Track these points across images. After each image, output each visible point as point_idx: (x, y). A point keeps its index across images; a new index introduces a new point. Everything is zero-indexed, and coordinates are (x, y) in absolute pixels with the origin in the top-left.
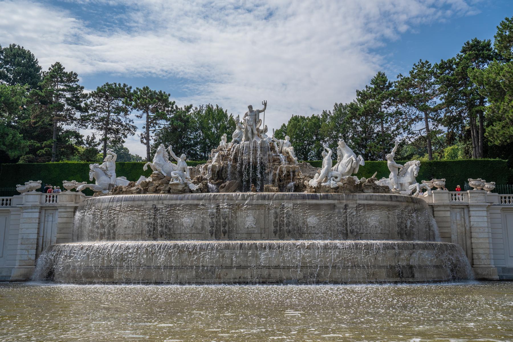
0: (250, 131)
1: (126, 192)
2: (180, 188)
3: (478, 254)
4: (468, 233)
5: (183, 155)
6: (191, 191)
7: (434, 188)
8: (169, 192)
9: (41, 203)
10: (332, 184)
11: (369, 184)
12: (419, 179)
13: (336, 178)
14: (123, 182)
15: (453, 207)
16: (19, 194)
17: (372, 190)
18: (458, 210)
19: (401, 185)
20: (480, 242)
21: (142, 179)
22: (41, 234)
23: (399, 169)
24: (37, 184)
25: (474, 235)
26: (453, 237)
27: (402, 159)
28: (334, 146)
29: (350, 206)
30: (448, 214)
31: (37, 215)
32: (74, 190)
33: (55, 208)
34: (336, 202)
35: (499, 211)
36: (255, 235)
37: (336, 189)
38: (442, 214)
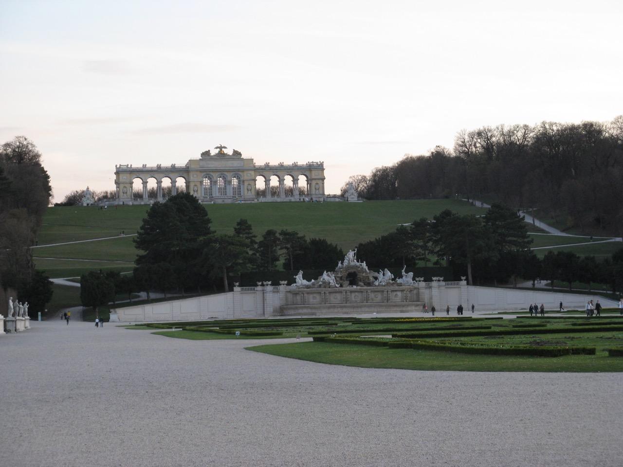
1: (312, 288)
4: (431, 298)
6: (336, 287)
7: (420, 281)
10: (384, 284)
12: (414, 279)
14: (305, 282)
16: (258, 286)
17: (396, 285)
21: (313, 281)
24: (270, 283)
28: (383, 271)
30: (424, 291)
32: (284, 285)
33: (278, 292)
37: (384, 286)
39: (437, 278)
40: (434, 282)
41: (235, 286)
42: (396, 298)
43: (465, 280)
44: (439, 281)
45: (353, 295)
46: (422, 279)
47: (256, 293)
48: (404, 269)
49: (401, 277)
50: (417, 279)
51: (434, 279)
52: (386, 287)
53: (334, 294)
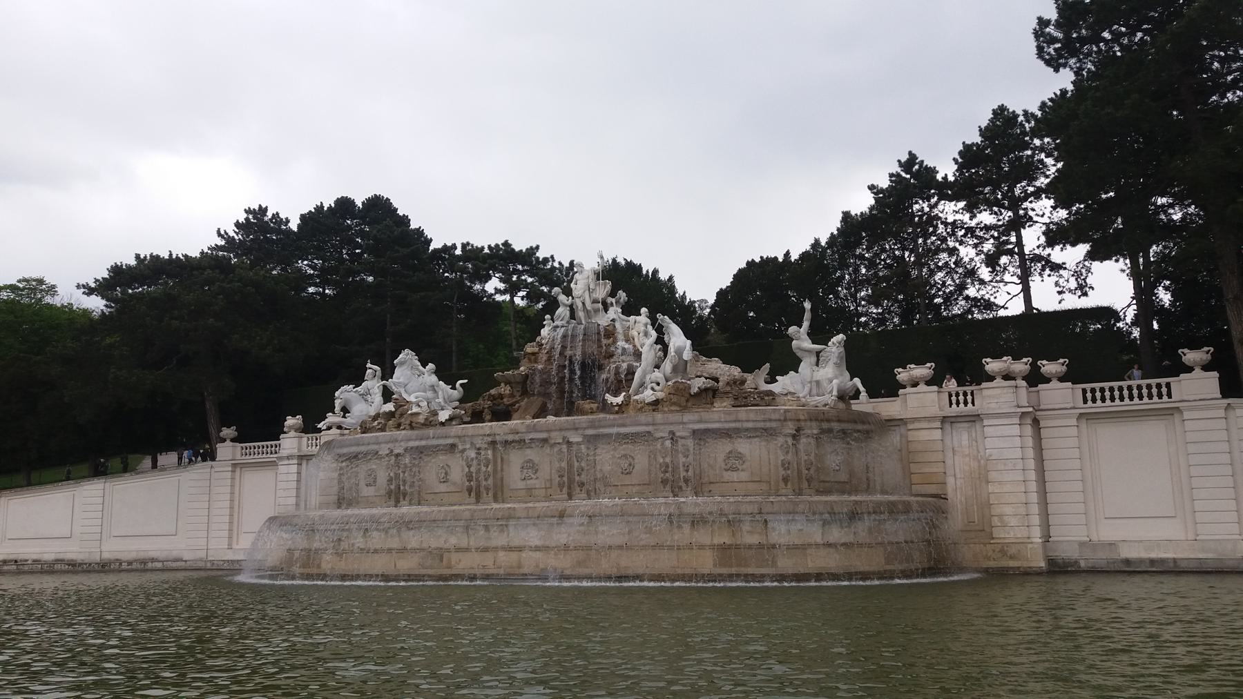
0: (580, 305)
2: (421, 419)
3: (1000, 516)
4: (981, 476)
5: (431, 366)
6: (442, 424)
8: (412, 428)
9: (299, 450)
10: (648, 395)
11: (728, 389)
13: (658, 384)
15: (944, 419)
18: (966, 425)
19: (818, 383)
20: (1005, 490)
22: (303, 498)
23: (818, 353)
25: (993, 475)
26: (950, 481)
27: (819, 335)
29: (678, 434)
30: (937, 434)
31: (294, 468)
34: (650, 428)
35: (1074, 422)
36: (536, 492)
37: (656, 403)
38: (924, 435)
39: (1022, 366)
40: (999, 382)
41: (224, 440)
42: (728, 476)
43: (1206, 368)
44: (1035, 378)
45: (515, 459)
46: (924, 371)
47: (273, 464)
48: (806, 324)
49: (789, 363)
50: (902, 375)
51: (992, 365)
52: (659, 417)
53: (442, 458)
